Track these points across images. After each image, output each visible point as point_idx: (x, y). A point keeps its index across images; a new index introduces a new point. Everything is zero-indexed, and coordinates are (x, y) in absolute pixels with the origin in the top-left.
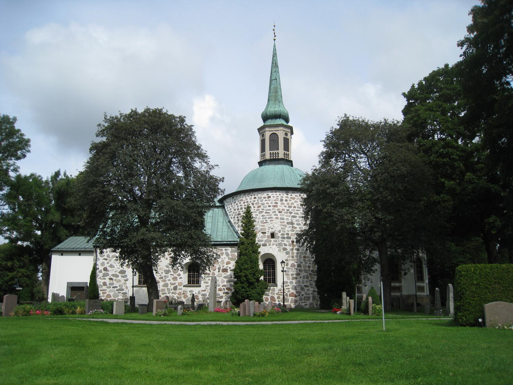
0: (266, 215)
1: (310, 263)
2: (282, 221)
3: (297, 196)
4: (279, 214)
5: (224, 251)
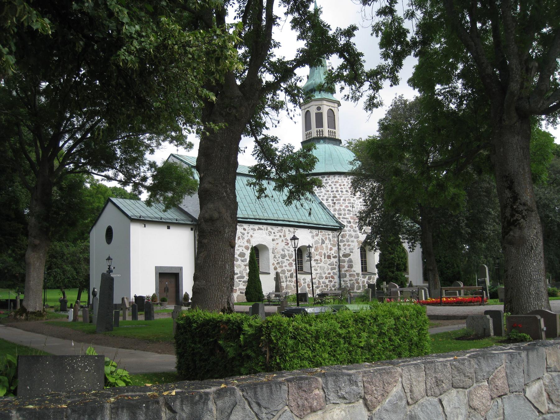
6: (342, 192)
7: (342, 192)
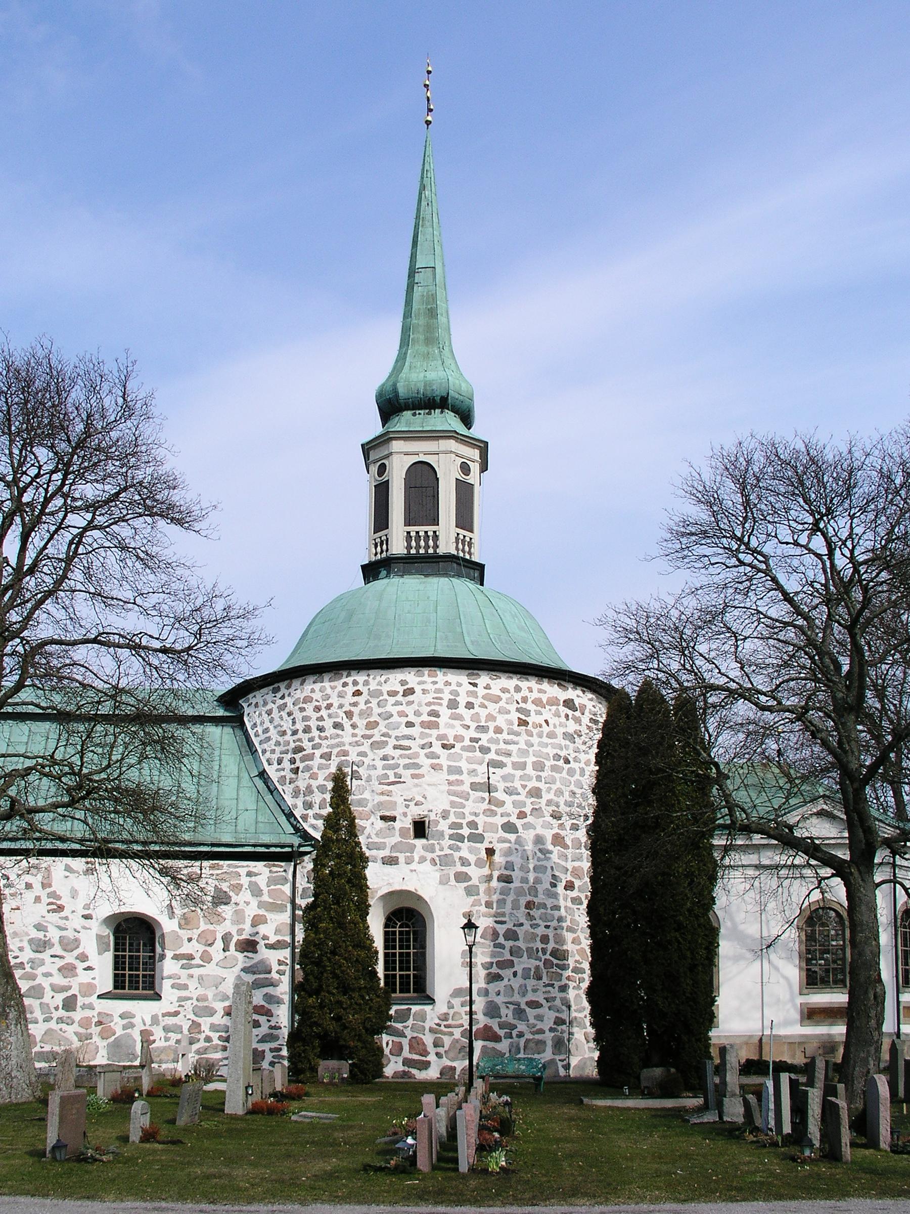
0: (396, 756)
1: (547, 927)
2: (453, 778)
3: (508, 691)
4: (444, 753)
5: (245, 881)
6: (321, 729)
7: (321, 729)
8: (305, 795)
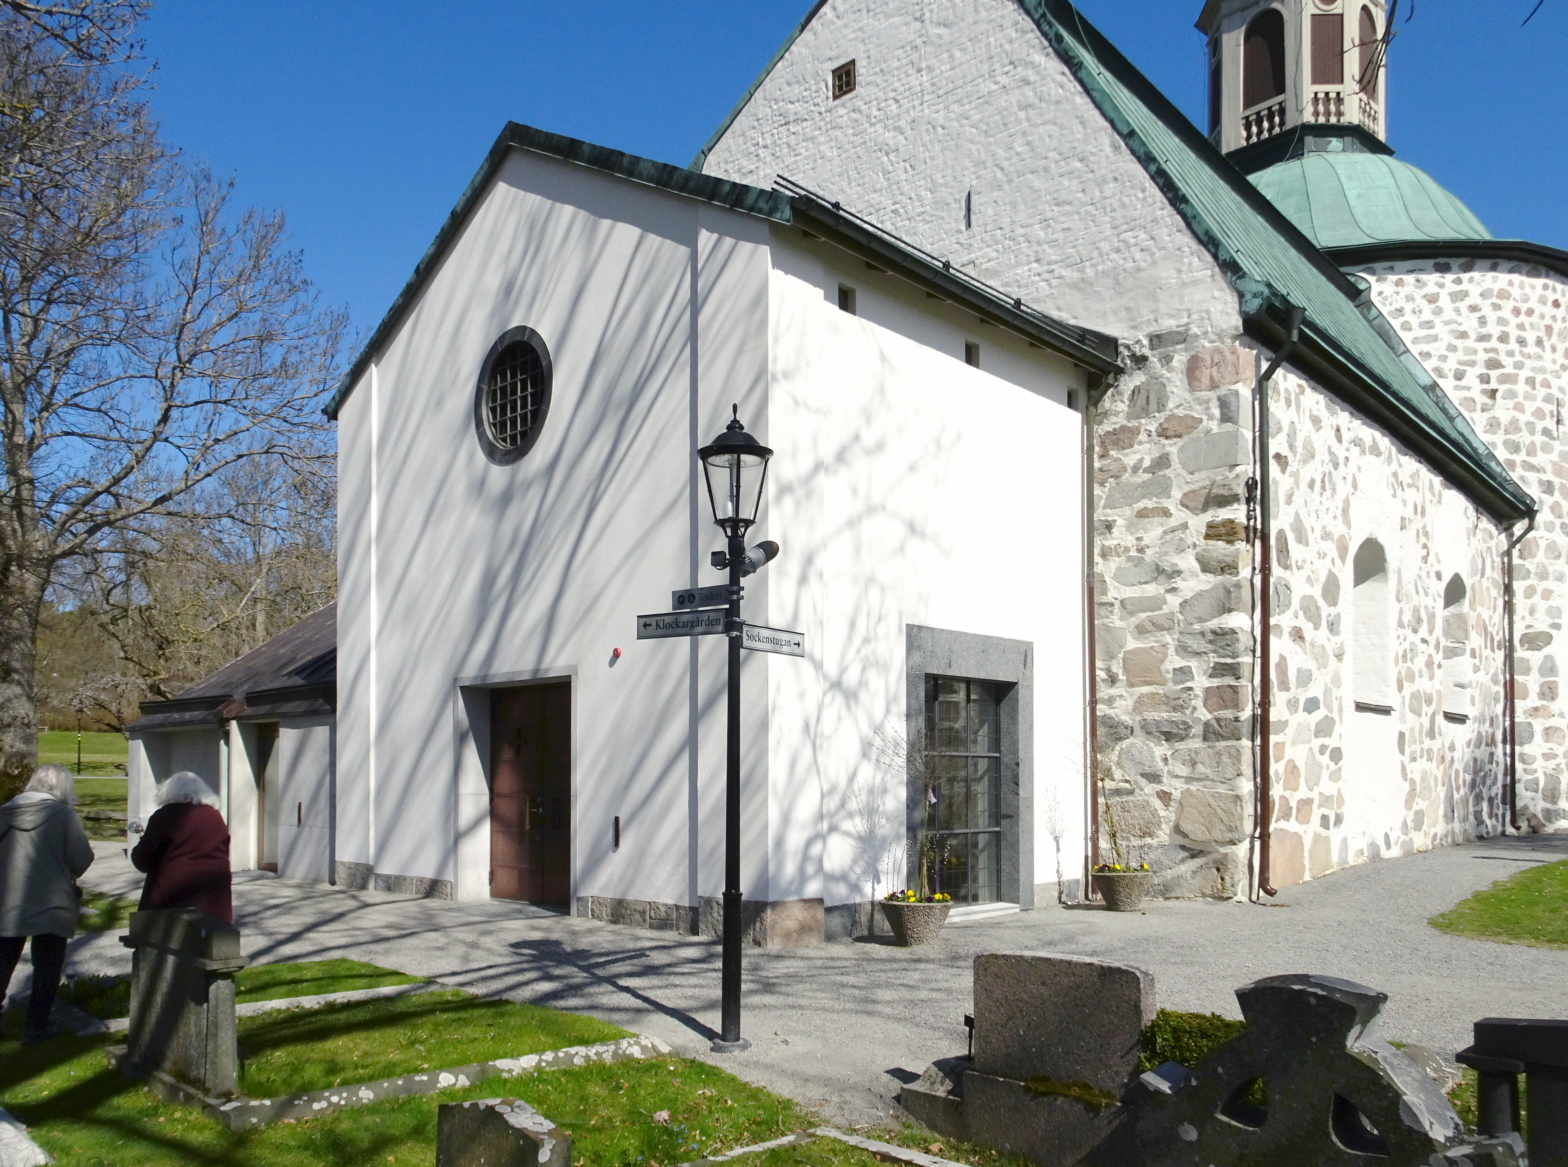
6: (1522, 342)
7: (1522, 342)
8: (1507, 432)
